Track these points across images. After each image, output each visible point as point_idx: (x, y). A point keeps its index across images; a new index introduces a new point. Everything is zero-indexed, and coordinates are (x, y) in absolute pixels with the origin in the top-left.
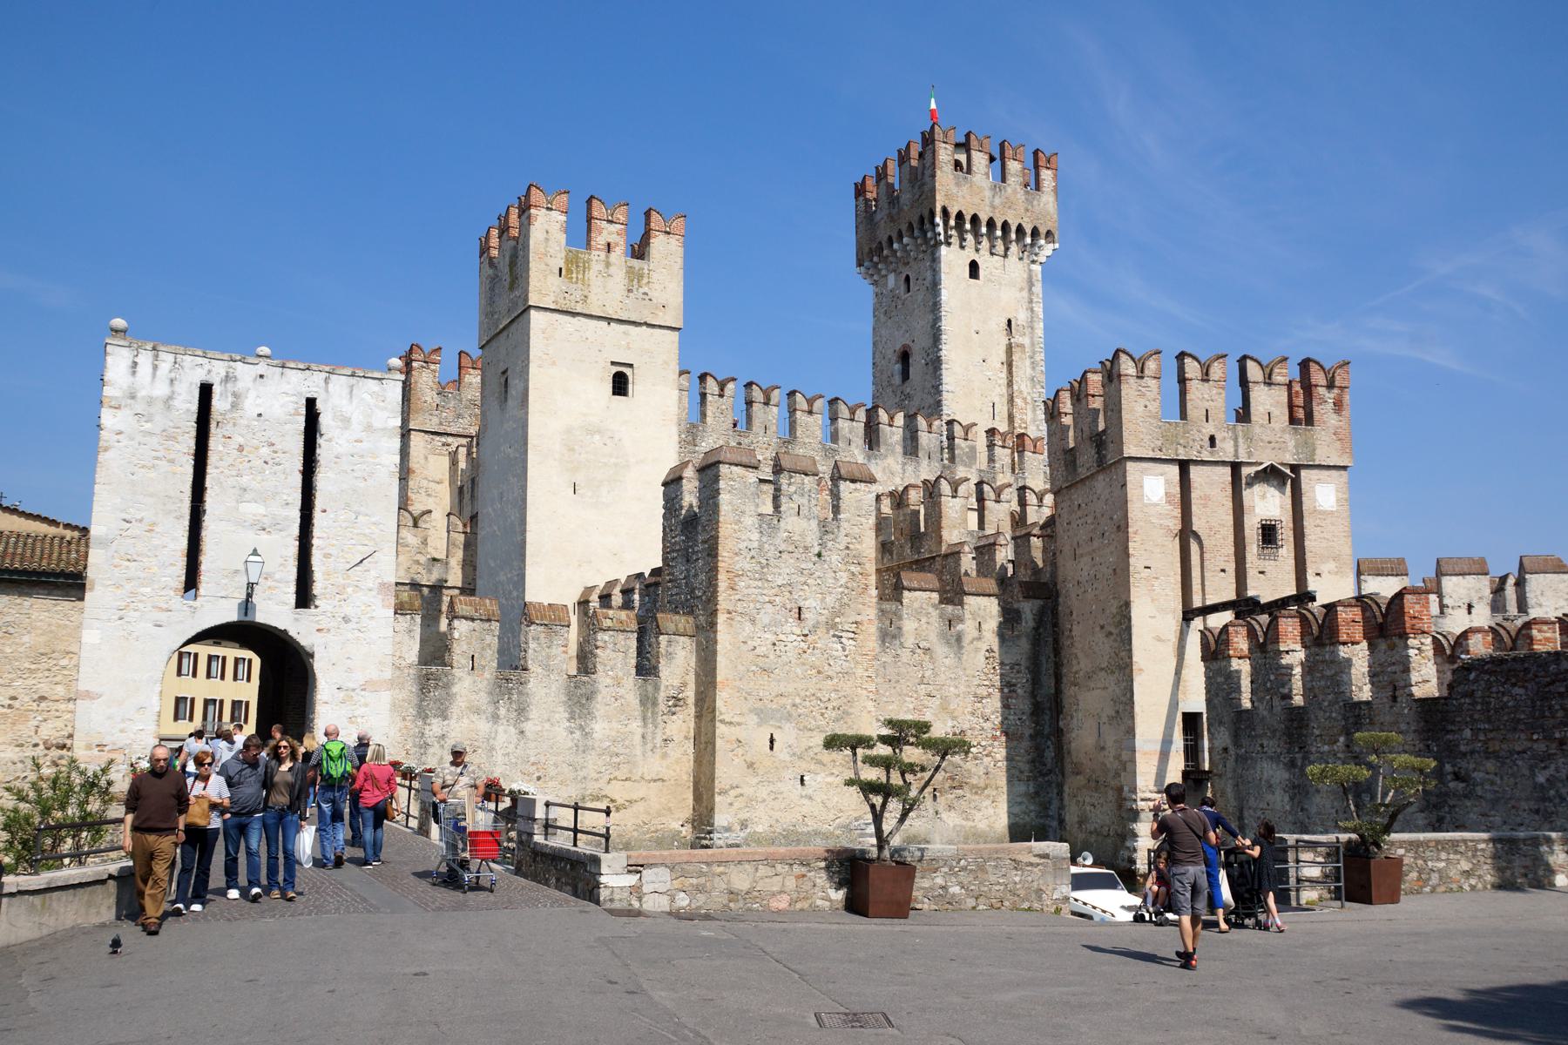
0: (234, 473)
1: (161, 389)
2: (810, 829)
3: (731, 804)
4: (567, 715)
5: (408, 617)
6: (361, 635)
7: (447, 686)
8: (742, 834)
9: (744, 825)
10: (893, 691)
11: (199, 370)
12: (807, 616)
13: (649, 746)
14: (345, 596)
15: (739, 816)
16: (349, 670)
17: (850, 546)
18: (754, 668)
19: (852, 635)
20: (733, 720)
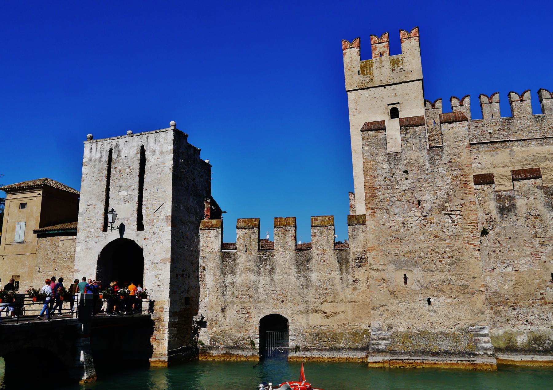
0: (118, 181)
1: (98, 155)
2: (437, 331)
3: (381, 315)
4: (296, 270)
5: (215, 230)
6: (159, 239)
7: (234, 260)
8: (389, 333)
9: (390, 327)
10: (513, 244)
11: (109, 145)
12: (424, 205)
13: (345, 284)
14: (153, 224)
15: (386, 322)
16: (155, 255)
17: (453, 161)
18: (391, 238)
19: (459, 212)
20: (379, 268)
